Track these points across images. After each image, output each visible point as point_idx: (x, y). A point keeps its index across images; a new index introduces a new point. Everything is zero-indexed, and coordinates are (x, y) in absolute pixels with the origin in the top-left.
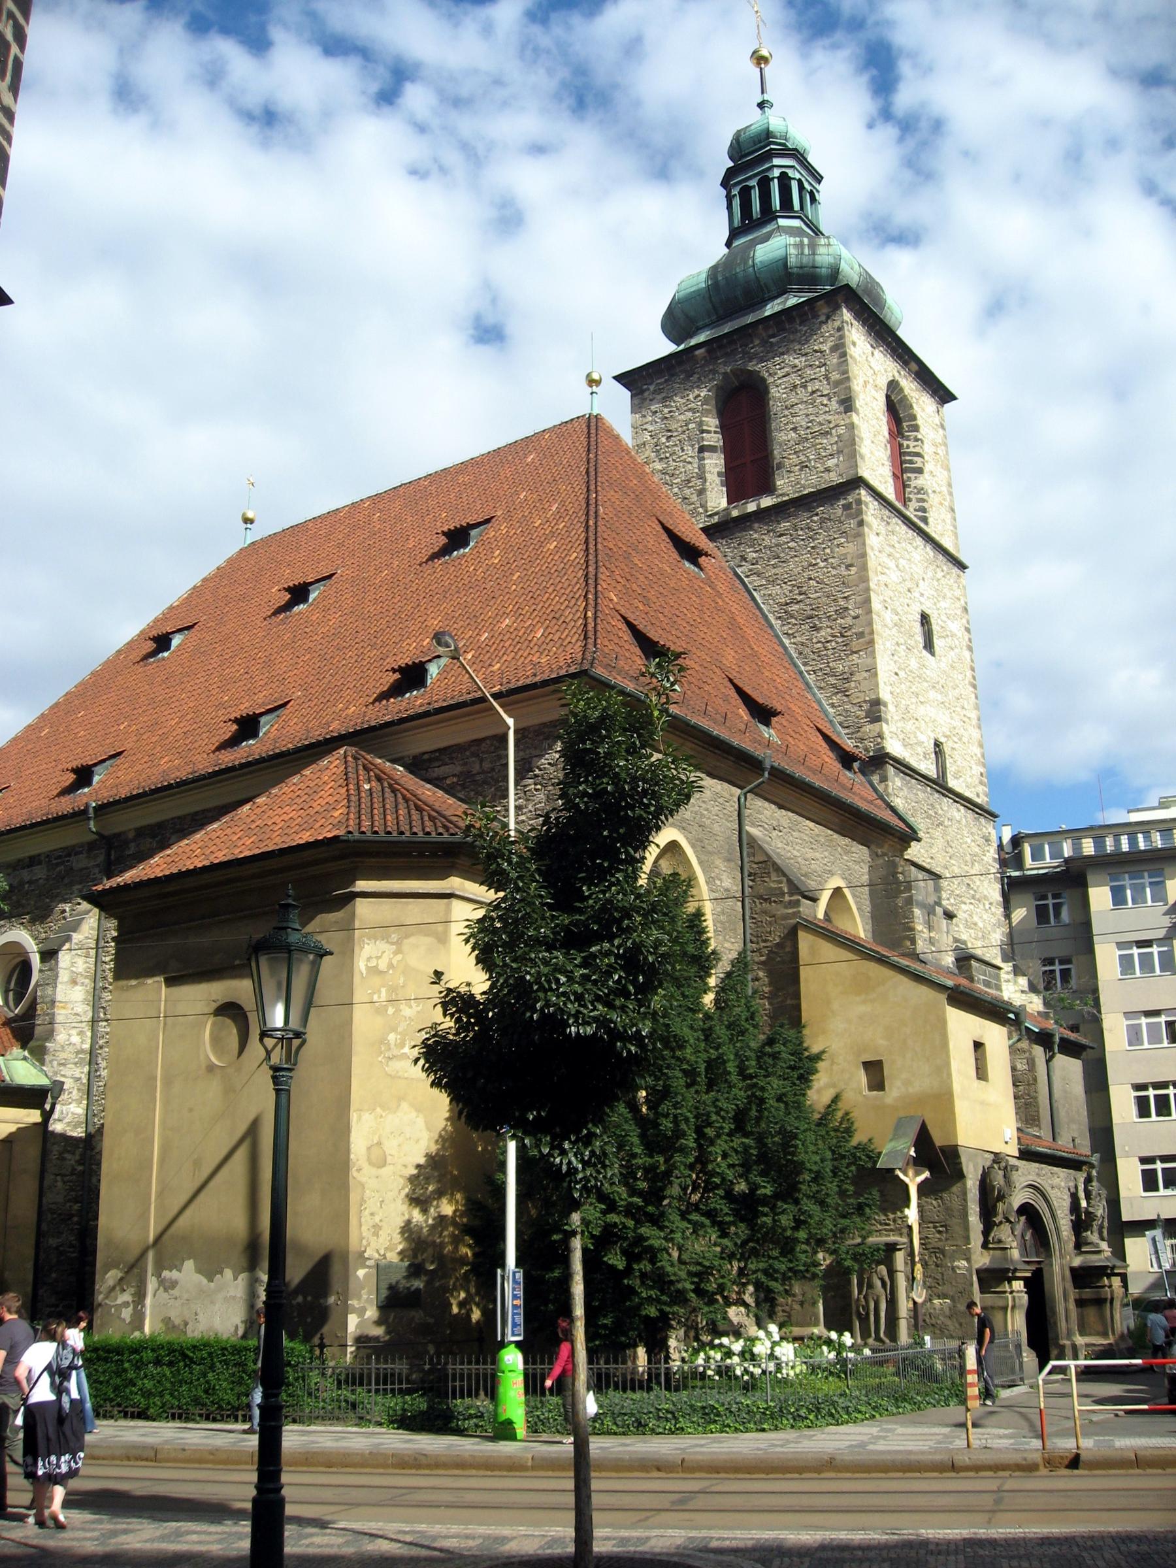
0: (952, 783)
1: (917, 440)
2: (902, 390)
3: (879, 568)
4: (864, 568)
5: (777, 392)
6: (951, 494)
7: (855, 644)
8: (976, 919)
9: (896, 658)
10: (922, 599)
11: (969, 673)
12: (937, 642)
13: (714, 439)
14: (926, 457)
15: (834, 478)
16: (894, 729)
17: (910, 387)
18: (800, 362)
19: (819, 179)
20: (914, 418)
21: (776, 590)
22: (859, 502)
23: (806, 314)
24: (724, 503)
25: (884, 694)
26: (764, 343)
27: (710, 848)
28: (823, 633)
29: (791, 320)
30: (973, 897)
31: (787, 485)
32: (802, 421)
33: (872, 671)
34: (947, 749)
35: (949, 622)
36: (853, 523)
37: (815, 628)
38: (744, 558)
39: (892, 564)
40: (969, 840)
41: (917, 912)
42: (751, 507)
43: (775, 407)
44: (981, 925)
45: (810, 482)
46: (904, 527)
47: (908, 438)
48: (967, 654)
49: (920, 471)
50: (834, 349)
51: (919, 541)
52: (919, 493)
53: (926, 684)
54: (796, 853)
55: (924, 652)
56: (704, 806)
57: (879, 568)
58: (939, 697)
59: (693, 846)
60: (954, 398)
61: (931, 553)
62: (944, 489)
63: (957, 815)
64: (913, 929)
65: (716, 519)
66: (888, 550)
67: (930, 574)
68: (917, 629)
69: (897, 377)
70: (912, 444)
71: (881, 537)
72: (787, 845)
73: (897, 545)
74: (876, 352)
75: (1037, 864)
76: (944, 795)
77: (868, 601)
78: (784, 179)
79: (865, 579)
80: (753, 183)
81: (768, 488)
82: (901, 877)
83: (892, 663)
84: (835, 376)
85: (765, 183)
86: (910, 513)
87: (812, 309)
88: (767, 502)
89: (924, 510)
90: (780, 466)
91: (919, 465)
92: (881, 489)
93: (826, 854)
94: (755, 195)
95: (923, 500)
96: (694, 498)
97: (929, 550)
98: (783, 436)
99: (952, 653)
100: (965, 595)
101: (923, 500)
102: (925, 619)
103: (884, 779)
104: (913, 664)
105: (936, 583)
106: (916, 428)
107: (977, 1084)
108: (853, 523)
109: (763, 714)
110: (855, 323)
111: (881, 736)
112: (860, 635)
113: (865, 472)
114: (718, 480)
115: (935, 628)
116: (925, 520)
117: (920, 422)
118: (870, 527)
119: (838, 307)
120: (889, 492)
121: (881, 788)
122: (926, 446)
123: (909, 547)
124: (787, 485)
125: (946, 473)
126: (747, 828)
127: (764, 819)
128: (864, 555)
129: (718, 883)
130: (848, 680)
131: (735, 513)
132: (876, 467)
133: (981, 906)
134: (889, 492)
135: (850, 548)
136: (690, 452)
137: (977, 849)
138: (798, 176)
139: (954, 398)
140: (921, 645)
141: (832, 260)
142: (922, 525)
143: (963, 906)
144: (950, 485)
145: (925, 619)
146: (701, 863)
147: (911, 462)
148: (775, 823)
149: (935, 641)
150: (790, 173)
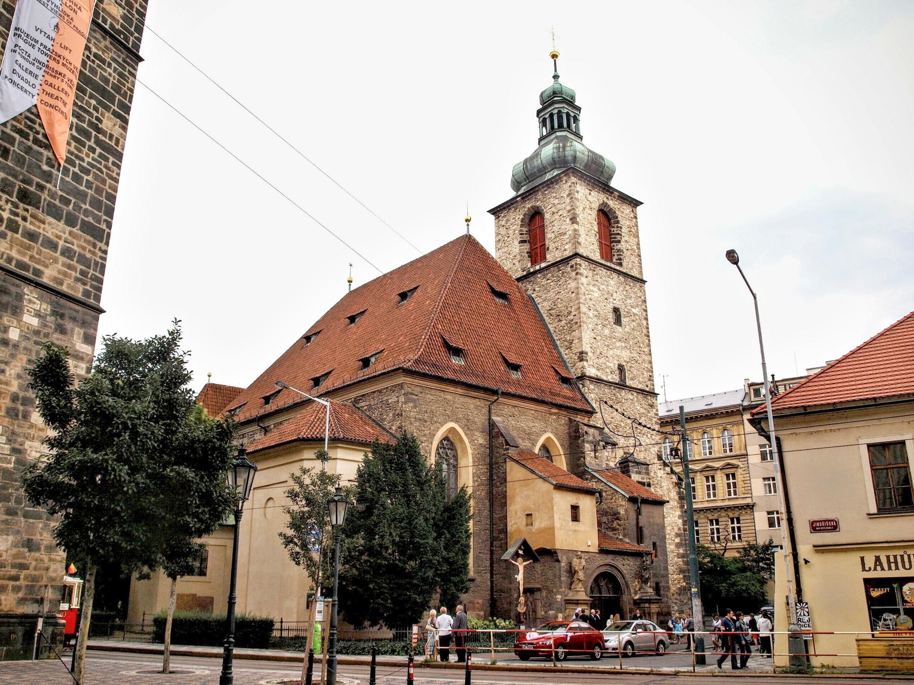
0: (629, 382)
4: (578, 294)
5: (547, 216)
6: (639, 248)
7: (575, 327)
11: (645, 331)
12: (624, 320)
13: (526, 237)
15: (568, 253)
16: (591, 363)
17: (613, 204)
18: (556, 202)
19: (579, 109)
21: (545, 304)
22: (576, 264)
24: (529, 265)
25: (586, 348)
26: (543, 193)
29: (552, 183)
31: (551, 257)
32: (555, 229)
33: (580, 339)
36: (574, 274)
39: (596, 289)
41: (587, 445)
42: (537, 267)
43: (547, 223)
46: (605, 271)
48: (644, 322)
49: (619, 242)
50: (569, 195)
51: (615, 275)
59: (463, 428)
61: (623, 280)
62: (635, 247)
63: (631, 397)
65: (525, 273)
66: (593, 283)
67: (621, 289)
69: (605, 200)
75: (758, 399)
77: (579, 308)
78: (560, 113)
79: (578, 299)
80: (547, 116)
81: (544, 258)
84: (569, 208)
85: (551, 116)
87: (560, 178)
88: (543, 265)
90: (548, 249)
92: (592, 256)
94: (555, 117)
96: (517, 263)
97: (622, 279)
98: (549, 235)
100: (645, 295)
102: (616, 310)
103: (584, 386)
104: (607, 332)
106: (618, 222)
107: (571, 523)
108: (574, 274)
112: (576, 323)
113: (581, 251)
115: (622, 313)
116: (621, 264)
118: (581, 274)
119: (569, 177)
120: (597, 256)
121: (583, 390)
123: (607, 279)
124: (551, 257)
126: (494, 418)
128: (578, 288)
130: (571, 343)
131: (532, 270)
132: (590, 246)
134: (597, 256)
135: (573, 285)
136: (516, 243)
137: (644, 411)
138: (566, 111)
141: (572, 152)
142: (618, 268)
144: (638, 244)
145: (616, 310)
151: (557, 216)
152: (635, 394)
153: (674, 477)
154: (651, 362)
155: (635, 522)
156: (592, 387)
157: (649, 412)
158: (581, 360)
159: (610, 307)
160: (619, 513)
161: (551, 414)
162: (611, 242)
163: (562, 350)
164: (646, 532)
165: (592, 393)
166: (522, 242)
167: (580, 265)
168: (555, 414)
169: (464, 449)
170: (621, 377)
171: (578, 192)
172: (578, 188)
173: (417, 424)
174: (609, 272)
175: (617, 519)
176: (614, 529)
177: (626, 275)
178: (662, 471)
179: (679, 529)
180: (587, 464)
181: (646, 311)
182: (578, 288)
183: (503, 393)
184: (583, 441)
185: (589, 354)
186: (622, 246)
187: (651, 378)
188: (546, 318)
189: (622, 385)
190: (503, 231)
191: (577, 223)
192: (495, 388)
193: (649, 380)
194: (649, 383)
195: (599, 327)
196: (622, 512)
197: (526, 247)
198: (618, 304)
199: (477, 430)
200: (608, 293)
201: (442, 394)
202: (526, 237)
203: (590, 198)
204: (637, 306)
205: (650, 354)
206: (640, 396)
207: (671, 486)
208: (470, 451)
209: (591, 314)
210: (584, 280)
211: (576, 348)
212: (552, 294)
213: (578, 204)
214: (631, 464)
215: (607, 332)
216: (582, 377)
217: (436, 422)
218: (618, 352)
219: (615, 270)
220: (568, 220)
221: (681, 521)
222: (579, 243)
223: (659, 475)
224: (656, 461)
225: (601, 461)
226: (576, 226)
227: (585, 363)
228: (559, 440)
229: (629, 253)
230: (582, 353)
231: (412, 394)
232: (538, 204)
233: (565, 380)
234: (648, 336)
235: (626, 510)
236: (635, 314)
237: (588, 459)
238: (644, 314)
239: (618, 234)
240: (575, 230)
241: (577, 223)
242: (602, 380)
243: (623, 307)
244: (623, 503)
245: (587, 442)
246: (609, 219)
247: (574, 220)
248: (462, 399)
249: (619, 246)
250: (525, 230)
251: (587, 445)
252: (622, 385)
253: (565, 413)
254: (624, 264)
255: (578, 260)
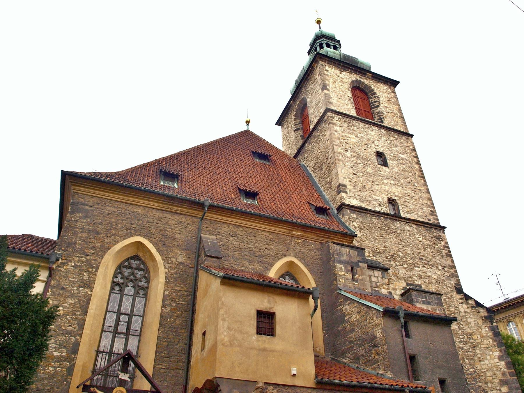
0: (403, 215)
1: (375, 97)
2: (363, 83)
3: (342, 138)
8: (429, 274)
9: (354, 168)
10: (376, 147)
14: (381, 102)
19: (339, 42)
20: (373, 90)
22: (328, 117)
23: (311, 71)
25: (343, 180)
27: (170, 245)
28: (324, 170)
29: (309, 75)
30: (426, 264)
33: (337, 175)
34: (400, 202)
35: (401, 155)
37: (322, 169)
38: (304, 158)
39: (353, 136)
40: (421, 239)
41: (339, 266)
44: (434, 276)
45: (316, 121)
46: (362, 124)
47: (371, 98)
48: (417, 167)
49: (378, 106)
52: (378, 113)
53: (380, 178)
54: (250, 246)
55: (379, 166)
56: (168, 227)
57: (341, 138)
58: (392, 182)
59: (154, 244)
60: (398, 82)
61: (385, 132)
63: (409, 228)
64: (336, 274)
66: (349, 131)
68: (374, 158)
69: (358, 78)
70: (373, 99)
71: (343, 128)
72: (244, 243)
73: (356, 130)
74: (344, 73)
76: (396, 220)
82: (331, 251)
83: (352, 170)
86: (376, 121)
87: (313, 68)
89: (381, 119)
91: (377, 104)
93: (280, 246)
95: (380, 115)
99: (404, 166)
101: (380, 115)
105: (389, 142)
106: (375, 93)
108: (327, 125)
109: (252, 195)
110: (326, 64)
111: (342, 198)
113: (333, 108)
114: (300, 138)
116: (382, 122)
117: (376, 90)
118: (335, 124)
120: (353, 113)
121: (343, 220)
122: (381, 99)
124: (312, 127)
125: (397, 107)
127: (222, 231)
129: (174, 260)
130: (331, 183)
133: (435, 268)
134: (353, 113)
136: (293, 133)
137: (429, 243)
139: (398, 82)
140: (377, 164)
143: (416, 268)
145: (380, 155)
146: (159, 251)
147: (374, 105)
148: (231, 233)
149: (388, 161)
150: (322, 42)
151: (314, 95)
152: (414, 226)
153: (481, 310)
154: (430, 199)
155: (401, 347)
156: (354, 216)
157: (435, 244)
158: (339, 192)
159: (372, 151)
160: (376, 337)
161: (294, 237)
162: (371, 109)
163: (324, 193)
164: (421, 360)
165: (353, 222)
166: (296, 130)
167: (333, 117)
168: (299, 237)
169: (156, 267)
170: (395, 211)
171: (327, 71)
172: (327, 68)
173: (85, 235)
174: (367, 126)
175: (375, 346)
176: (375, 362)
177: (389, 129)
178: (465, 306)
179: (503, 374)
180: (340, 287)
181: (417, 157)
182: (331, 134)
183: (211, 207)
184: (334, 262)
185: (348, 187)
186: (381, 108)
187: (433, 213)
188: (313, 174)
189: (397, 217)
190: (286, 131)
191: (328, 90)
192: (202, 200)
193: (431, 215)
194: (431, 217)
195: (360, 166)
196: (379, 335)
197: (300, 133)
198: (380, 150)
199: (178, 246)
200: (369, 140)
201: (130, 208)
202: (299, 126)
203: (341, 75)
204: (405, 153)
205: (429, 193)
206: (421, 229)
207: (480, 322)
208: (162, 270)
209: (348, 154)
210: (337, 128)
211: (334, 185)
212: (315, 152)
213: (327, 78)
214: (413, 293)
215: (370, 170)
216: (342, 207)
217: (115, 235)
218: (387, 188)
219: (374, 124)
220: (320, 91)
221: (503, 363)
222: (331, 103)
223: (462, 310)
224: (454, 294)
225: (364, 285)
226: (325, 91)
227: (343, 194)
228: (306, 265)
229: (389, 115)
230: (340, 185)
231: (84, 204)
232: (302, 97)
233: (321, 211)
234: (424, 178)
235: (383, 331)
236: (403, 159)
237: (341, 282)
238: (415, 160)
239: (377, 101)
240: (325, 94)
241: (328, 90)
242: (367, 210)
243: (389, 152)
244: (378, 321)
245: (340, 262)
246: (366, 94)
247: (324, 87)
248: (158, 214)
249: (378, 110)
250: (298, 121)
251: (339, 266)
252: (397, 217)
253: (314, 237)
254: (385, 122)
255: (329, 114)
